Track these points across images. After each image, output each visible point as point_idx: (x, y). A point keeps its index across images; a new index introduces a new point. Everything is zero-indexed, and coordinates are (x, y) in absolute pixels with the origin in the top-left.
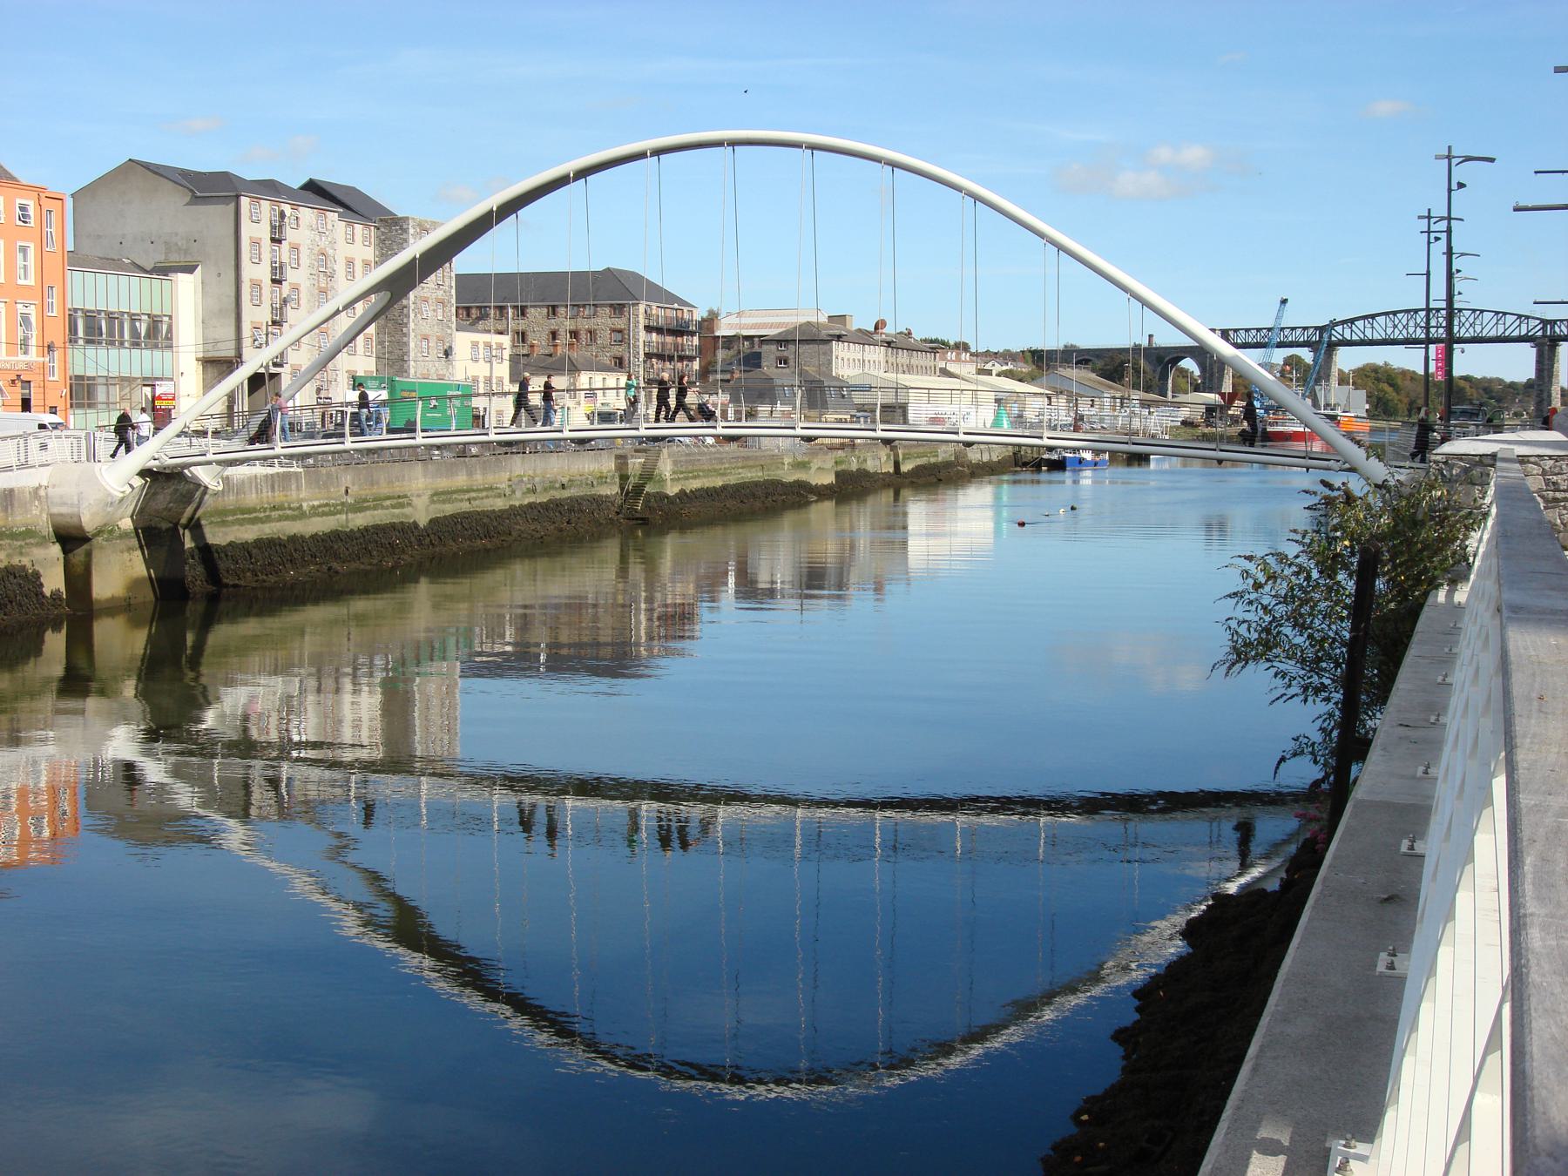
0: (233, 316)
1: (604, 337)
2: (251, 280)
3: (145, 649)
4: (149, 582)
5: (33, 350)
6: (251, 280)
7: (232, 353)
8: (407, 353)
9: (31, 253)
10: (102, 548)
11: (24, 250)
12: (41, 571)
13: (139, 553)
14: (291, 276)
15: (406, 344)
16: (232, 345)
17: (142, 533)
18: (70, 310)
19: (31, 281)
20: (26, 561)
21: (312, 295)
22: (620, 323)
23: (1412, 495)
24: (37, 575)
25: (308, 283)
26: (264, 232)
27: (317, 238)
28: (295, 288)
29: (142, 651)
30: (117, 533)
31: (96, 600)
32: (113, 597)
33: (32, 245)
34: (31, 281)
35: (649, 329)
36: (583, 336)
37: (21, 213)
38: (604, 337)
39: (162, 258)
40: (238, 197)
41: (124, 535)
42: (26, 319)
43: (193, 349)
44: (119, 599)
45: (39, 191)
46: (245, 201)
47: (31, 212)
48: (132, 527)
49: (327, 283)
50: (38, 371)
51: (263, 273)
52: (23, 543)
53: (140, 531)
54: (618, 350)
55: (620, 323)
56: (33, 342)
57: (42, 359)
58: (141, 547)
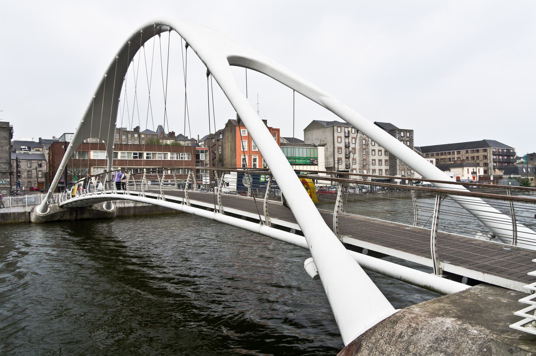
0: (333, 156)
1: (481, 158)
2: (338, 147)
6: (338, 147)
7: (332, 166)
8: (396, 164)
14: (352, 146)
15: (396, 162)
16: (333, 163)
21: (360, 150)
22: (485, 154)
23: (55, 351)
25: (359, 147)
26: (343, 135)
27: (362, 136)
28: (354, 149)
35: (494, 155)
36: (475, 158)
38: (481, 158)
39: (319, 143)
40: (333, 126)
43: (324, 164)
46: (335, 128)
49: (366, 147)
51: (342, 145)
54: (485, 161)
55: (485, 154)
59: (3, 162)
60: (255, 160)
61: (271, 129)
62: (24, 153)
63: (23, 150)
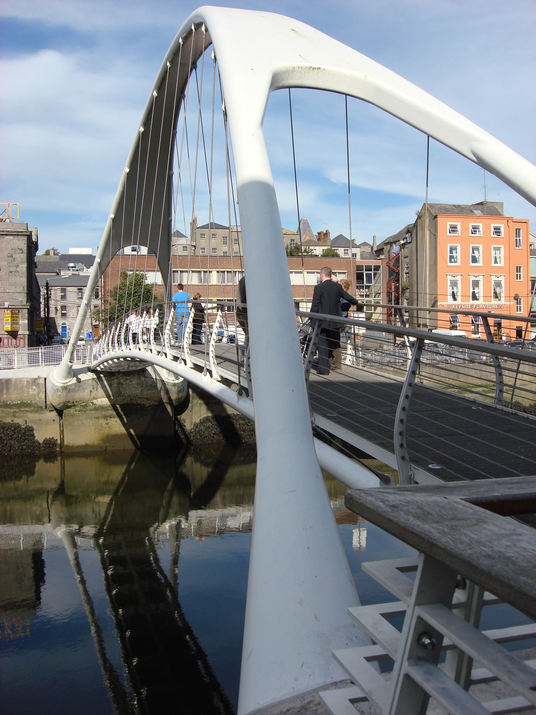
3: (123, 478)
4: (128, 438)
5: (503, 299)
9: (502, 250)
10: (73, 415)
11: (499, 249)
12: (35, 427)
13: (118, 420)
17: (120, 407)
18: (531, 277)
19: (502, 265)
20: (20, 421)
24: (31, 430)
29: (119, 478)
30: (91, 406)
31: (68, 446)
32: (87, 445)
33: (502, 247)
34: (502, 265)
37: (494, 231)
41: (102, 408)
42: (498, 284)
44: (93, 446)
45: (508, 220)
47: (502, 230)
48: (109, 403)
50: (505, 309)
52: (17, 410)
53: (118, 406)
56: (503, 294)
57: (509, 303)
58: (119, 416)
59: (19, 291)
60: (476, 284)
61: (510, 221)
62: (73, 274)
63: (71, 269)
